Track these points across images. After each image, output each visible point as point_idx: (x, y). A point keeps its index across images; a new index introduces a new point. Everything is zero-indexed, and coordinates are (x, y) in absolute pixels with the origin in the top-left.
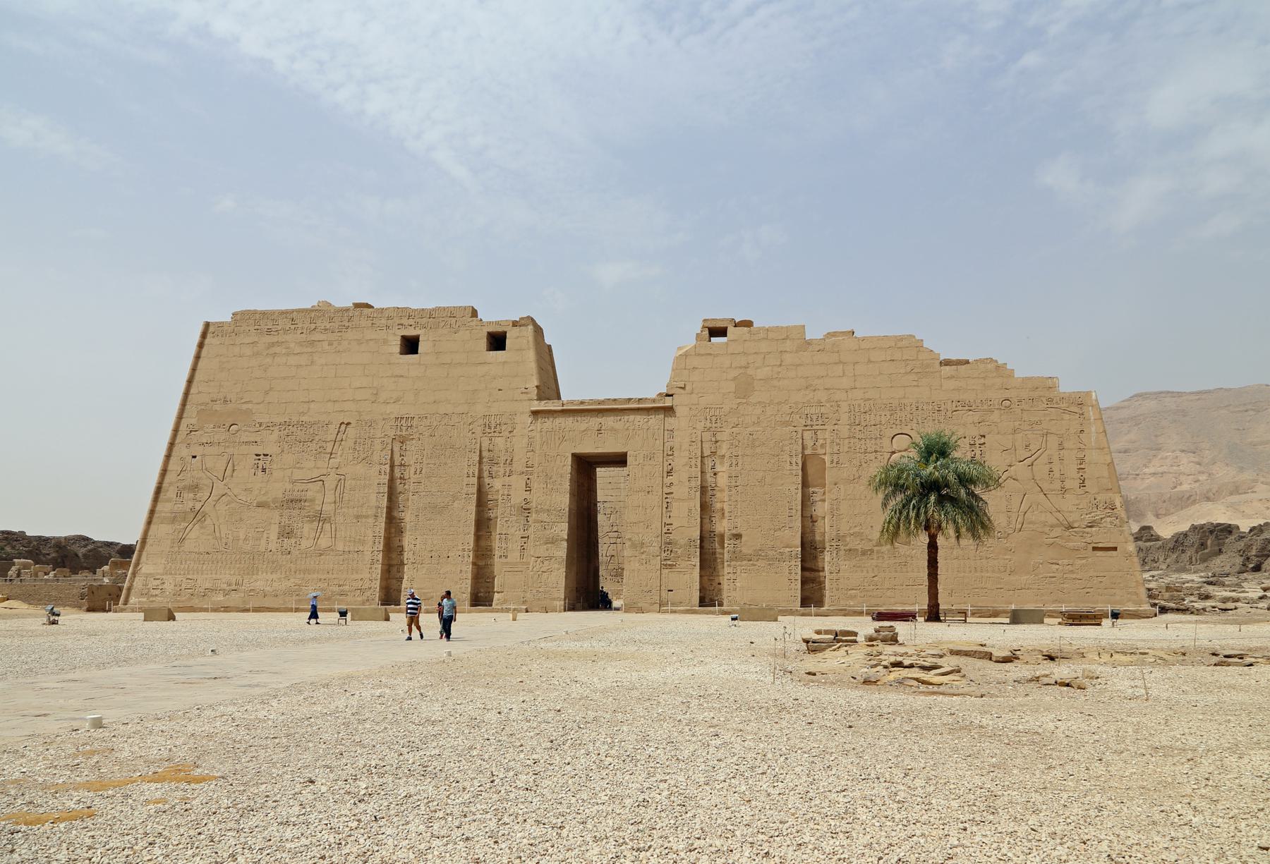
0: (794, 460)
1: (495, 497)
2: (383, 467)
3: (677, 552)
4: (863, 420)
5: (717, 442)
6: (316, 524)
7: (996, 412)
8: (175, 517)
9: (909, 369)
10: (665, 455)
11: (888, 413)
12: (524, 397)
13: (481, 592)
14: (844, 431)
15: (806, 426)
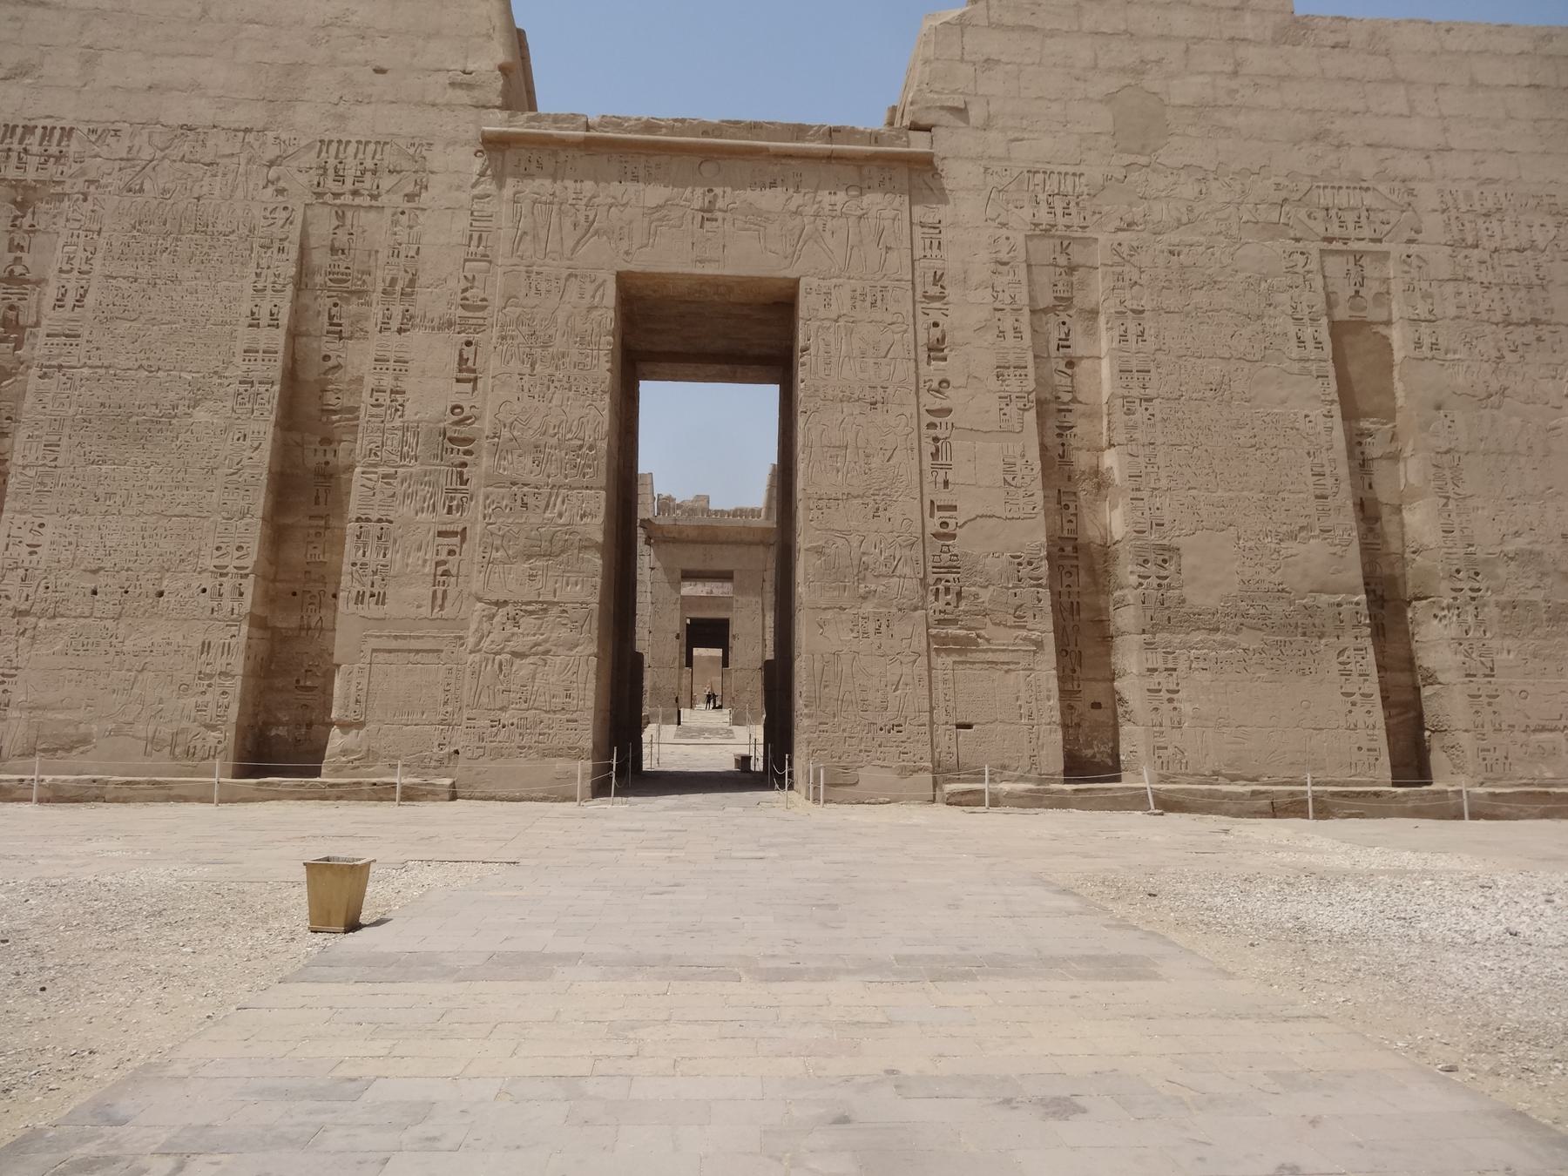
0: (1308, 332)
1: (346, 401)
3: (976, 596)
5: (1071, 269)
10: (919, 296)
12: (462, 96)
13: (278, 723)
15: (1330, 240)
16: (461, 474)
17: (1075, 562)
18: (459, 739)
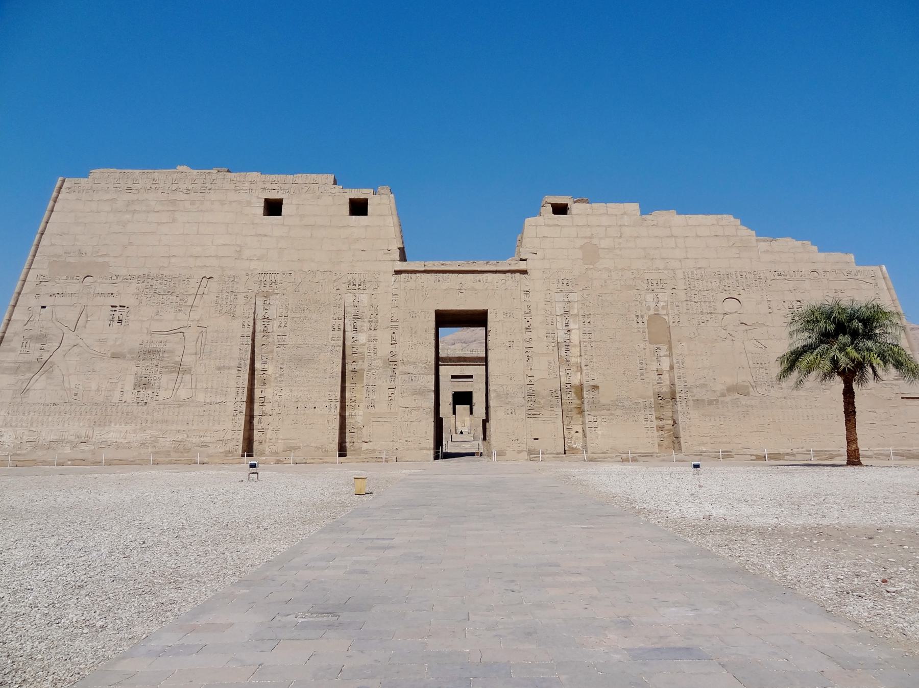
0: (640, 320)
1: (360, 350)
2: (246, 321)
4: (696, 285)
6: (175, 375)
7: (807, 281)
8: (18, 367)
9: (731, 244)
11: (718, 281)
14: (682, 296)
16: (394, 371)
17: (570, 390)
18: (396, 445)
